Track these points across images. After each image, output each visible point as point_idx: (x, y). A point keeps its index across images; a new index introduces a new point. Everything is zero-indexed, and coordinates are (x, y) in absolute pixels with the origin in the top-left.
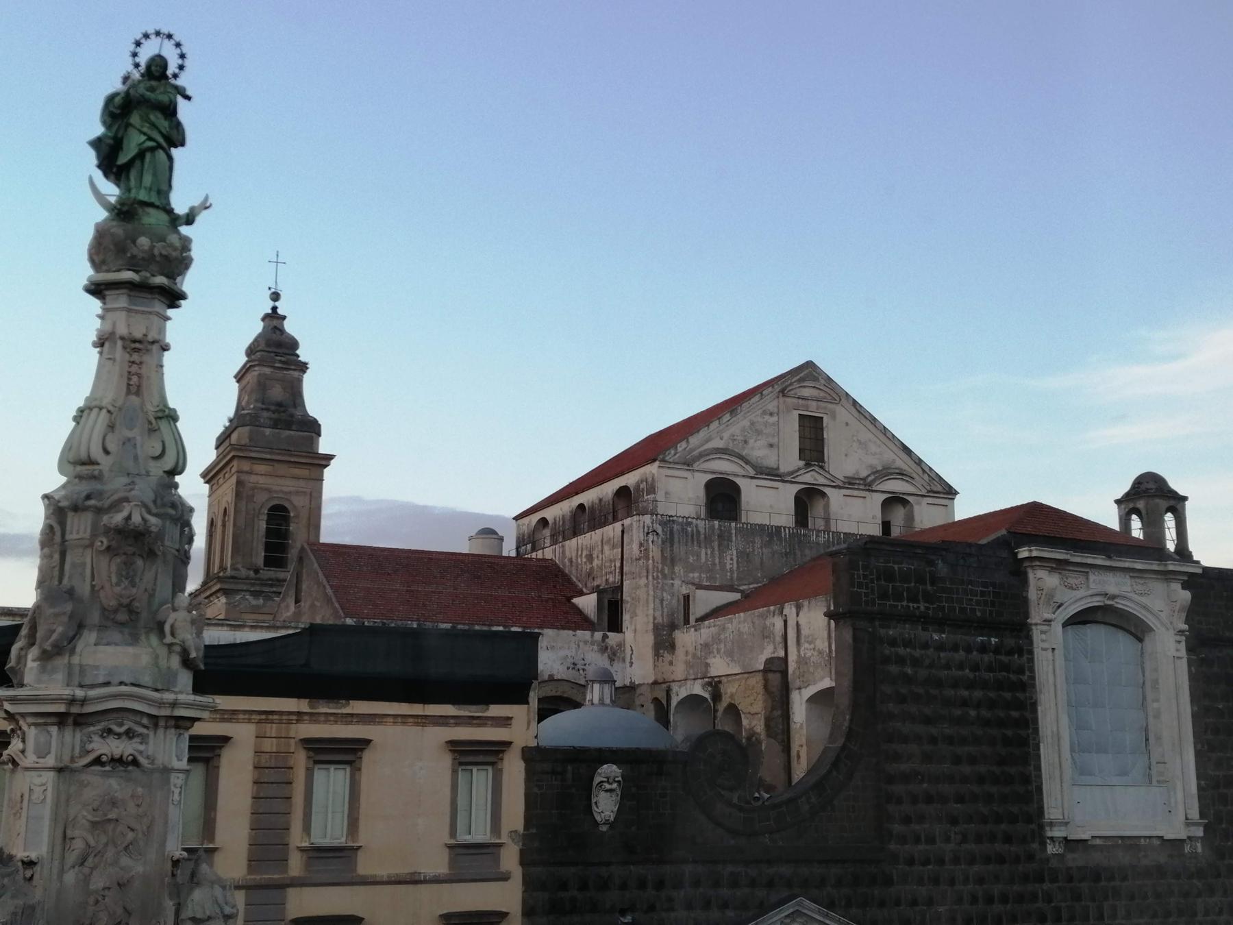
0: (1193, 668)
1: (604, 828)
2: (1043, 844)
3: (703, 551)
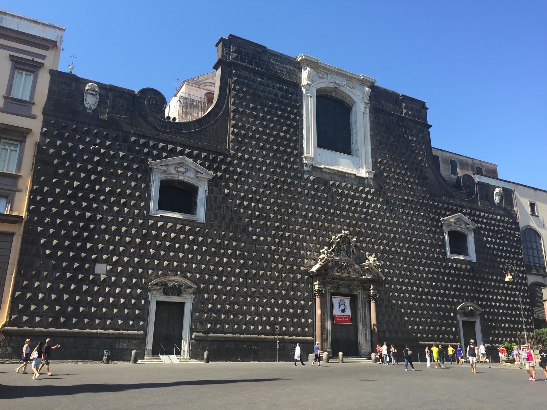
0: (372, 119)
1: (89, 111)
3: (200, 113)
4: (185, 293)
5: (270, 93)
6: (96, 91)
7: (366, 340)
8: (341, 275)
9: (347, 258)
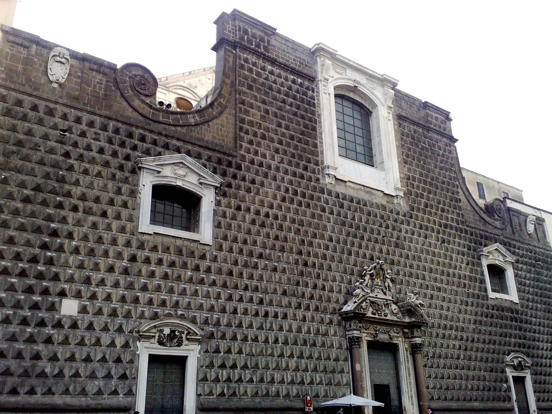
0: (396, 127)
1: (56, 85)
2: (323, 176)
4: (187, 342)
5: (282, 85)
6: (66, 59)
7: (413, 404)
8: (377, 316)
9: (383, 296)
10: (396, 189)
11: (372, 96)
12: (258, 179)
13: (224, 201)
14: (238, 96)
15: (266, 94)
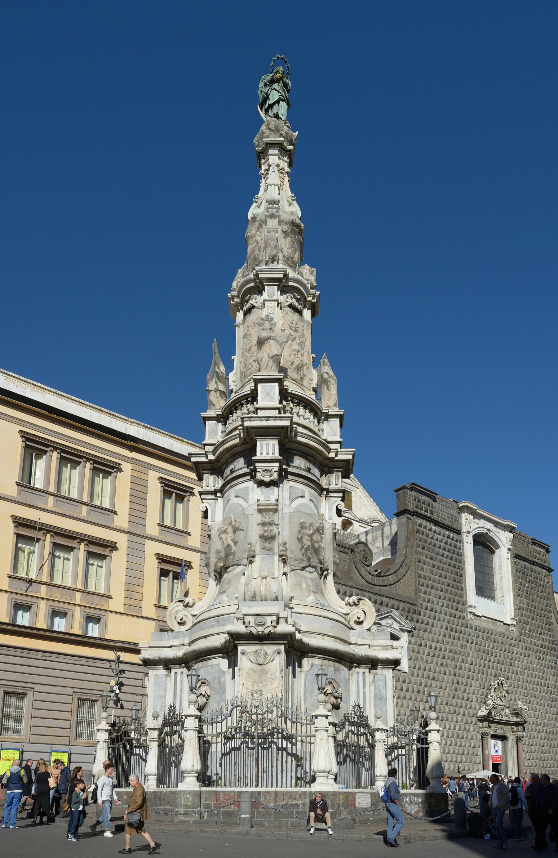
10: (512, 619)
11: (497, 540)
12: (430, 621)
13: (413, 640)
14: (416, 556)
15: (433, 551)
